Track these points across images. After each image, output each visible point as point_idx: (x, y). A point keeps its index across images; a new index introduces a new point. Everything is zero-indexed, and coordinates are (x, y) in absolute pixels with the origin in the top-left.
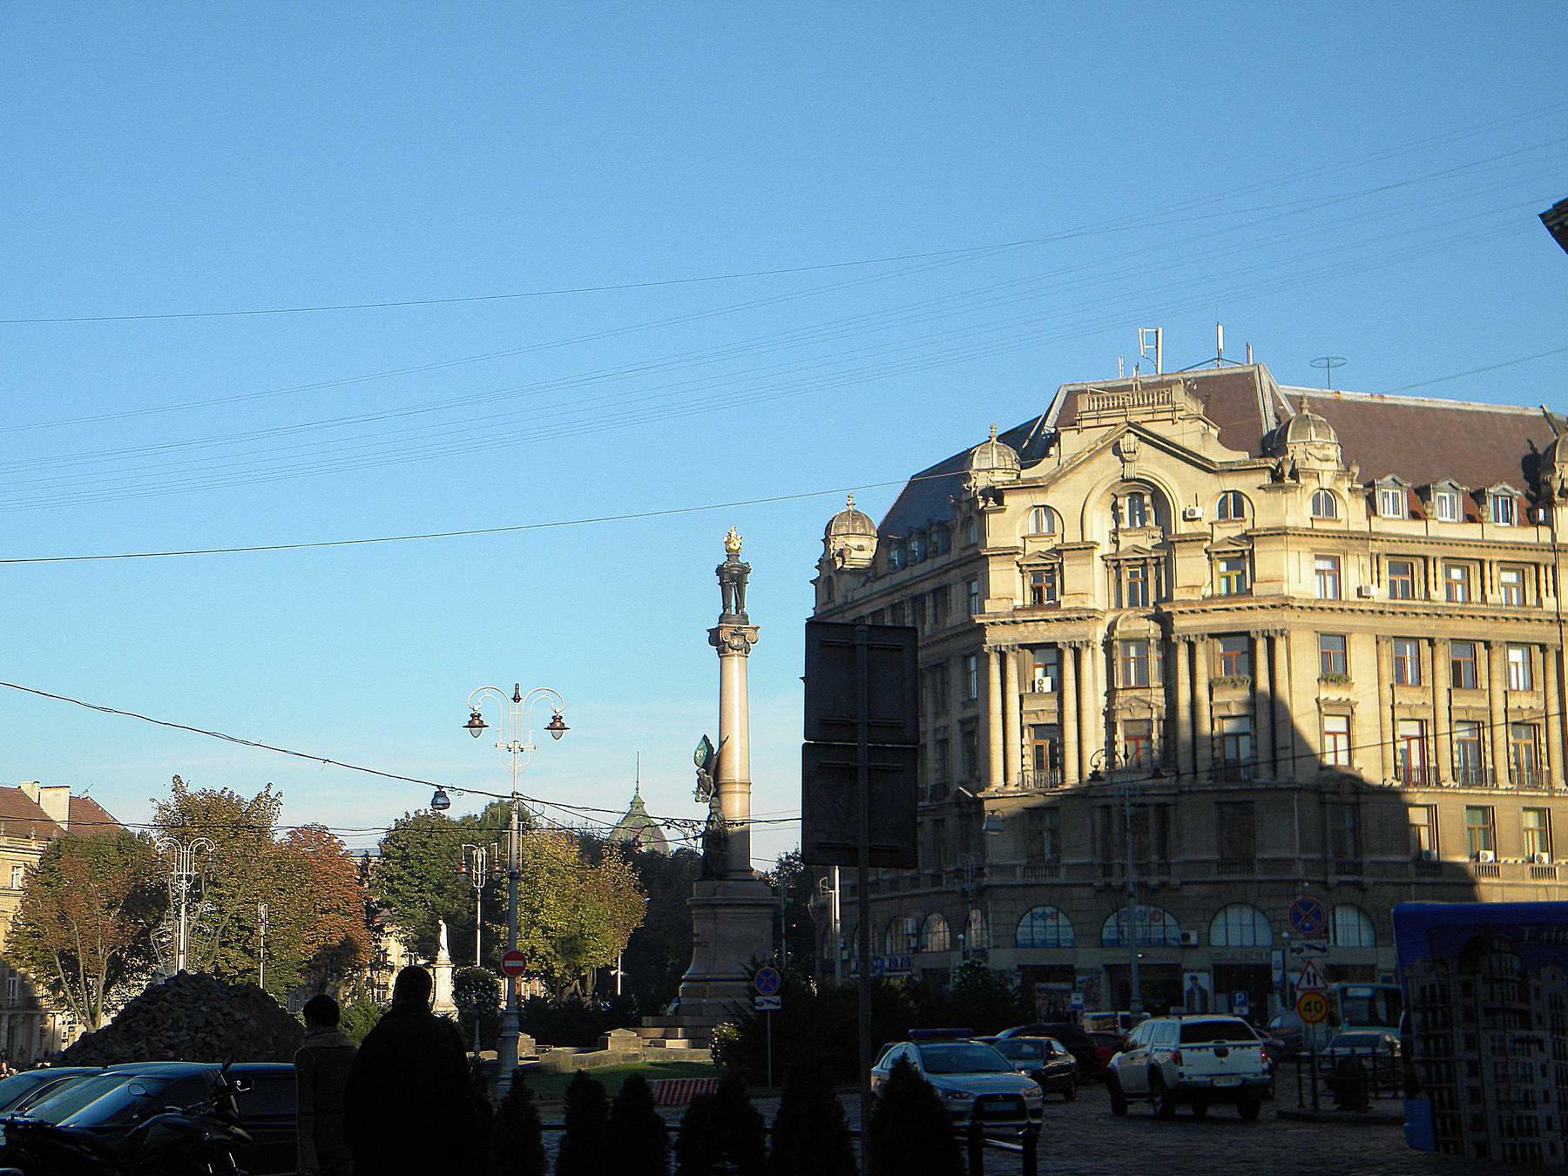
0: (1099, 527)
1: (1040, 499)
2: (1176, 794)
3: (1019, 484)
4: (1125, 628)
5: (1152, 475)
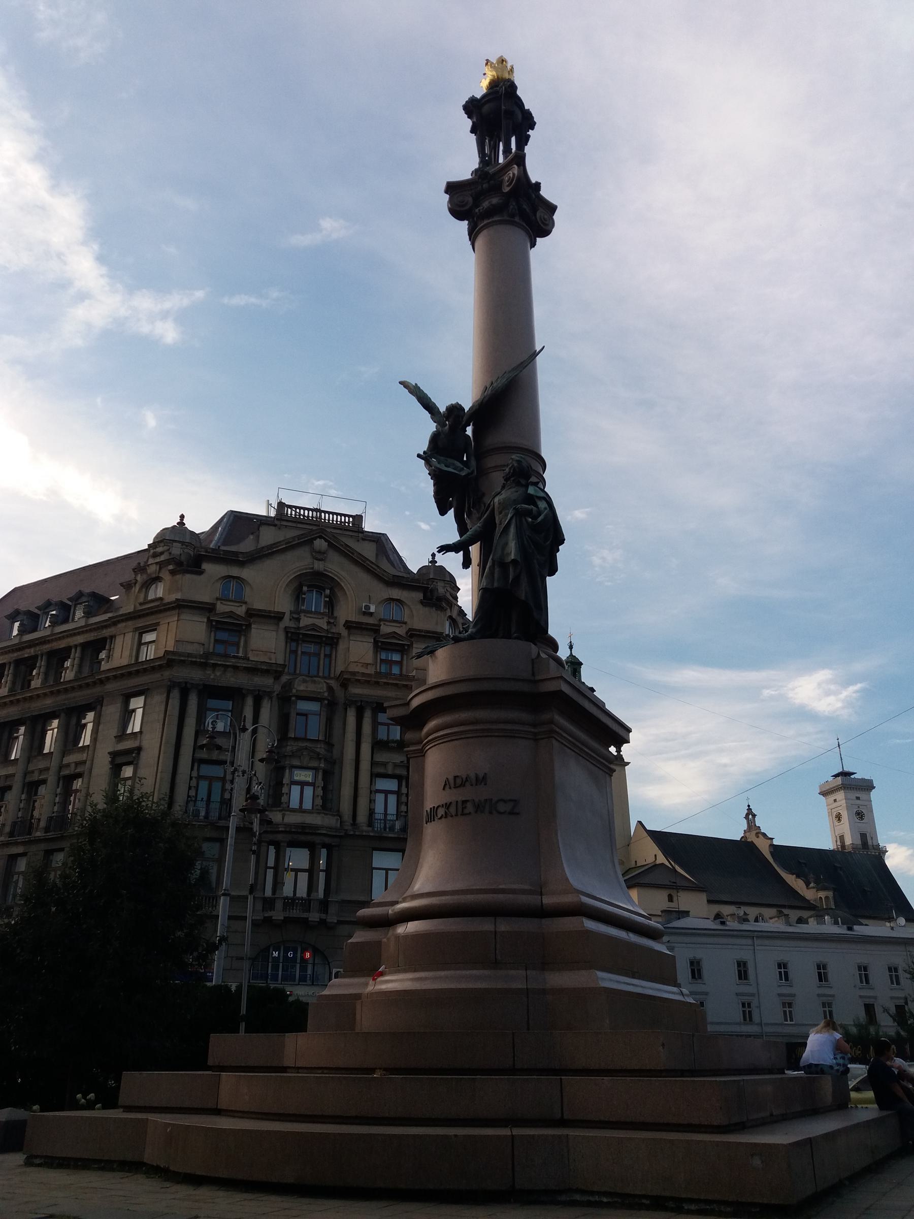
0: (283, 604)
1: (235, 571)
2: (341, 837)
3: (220, 554)
4: (302, 688)
5: (336, 573)
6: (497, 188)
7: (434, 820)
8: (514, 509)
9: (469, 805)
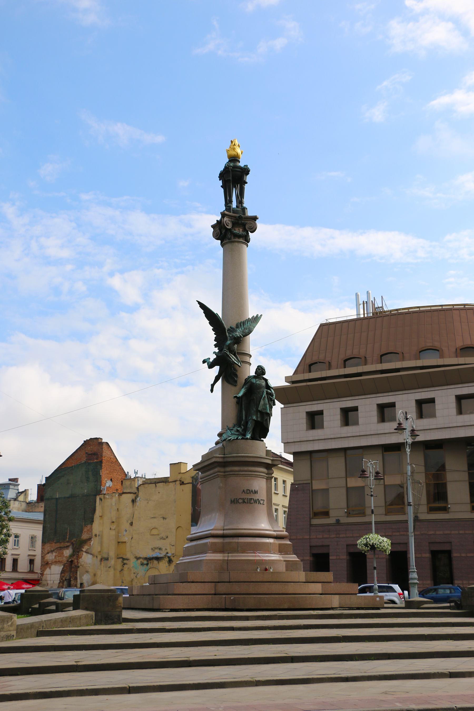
6: (244, 226)
7: (237, 503)
8: (266, 391)
9: (252, 500)
